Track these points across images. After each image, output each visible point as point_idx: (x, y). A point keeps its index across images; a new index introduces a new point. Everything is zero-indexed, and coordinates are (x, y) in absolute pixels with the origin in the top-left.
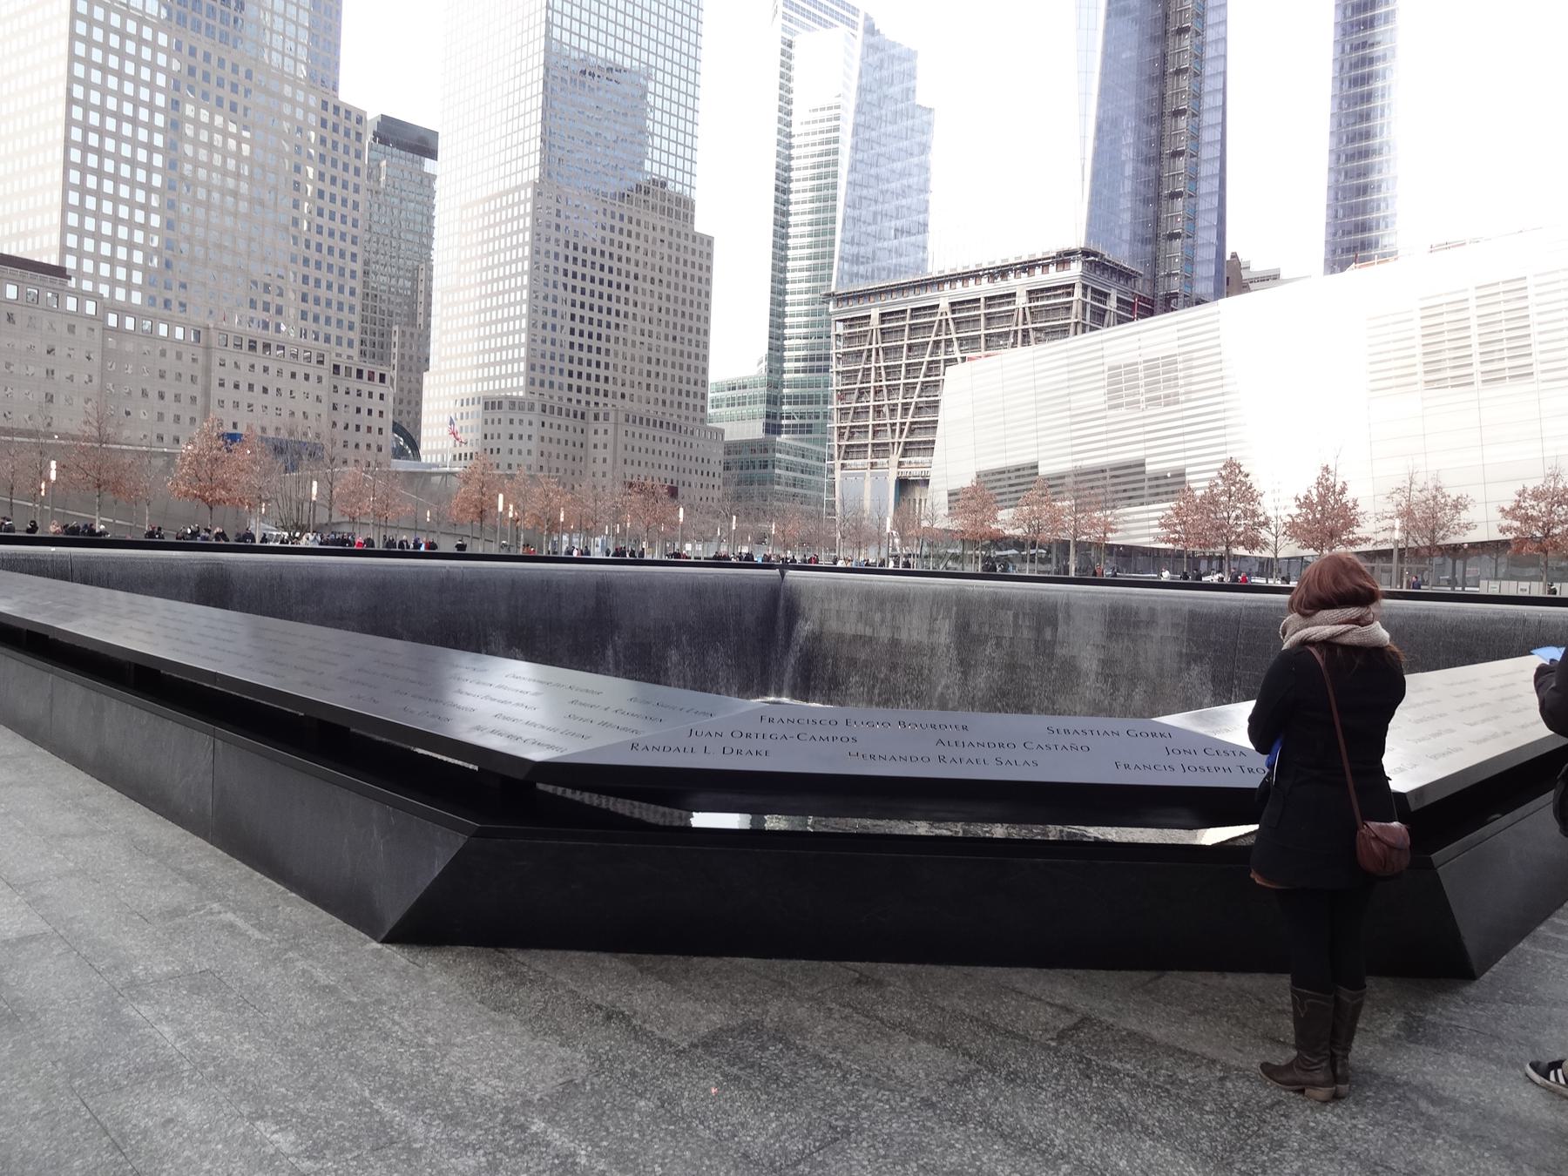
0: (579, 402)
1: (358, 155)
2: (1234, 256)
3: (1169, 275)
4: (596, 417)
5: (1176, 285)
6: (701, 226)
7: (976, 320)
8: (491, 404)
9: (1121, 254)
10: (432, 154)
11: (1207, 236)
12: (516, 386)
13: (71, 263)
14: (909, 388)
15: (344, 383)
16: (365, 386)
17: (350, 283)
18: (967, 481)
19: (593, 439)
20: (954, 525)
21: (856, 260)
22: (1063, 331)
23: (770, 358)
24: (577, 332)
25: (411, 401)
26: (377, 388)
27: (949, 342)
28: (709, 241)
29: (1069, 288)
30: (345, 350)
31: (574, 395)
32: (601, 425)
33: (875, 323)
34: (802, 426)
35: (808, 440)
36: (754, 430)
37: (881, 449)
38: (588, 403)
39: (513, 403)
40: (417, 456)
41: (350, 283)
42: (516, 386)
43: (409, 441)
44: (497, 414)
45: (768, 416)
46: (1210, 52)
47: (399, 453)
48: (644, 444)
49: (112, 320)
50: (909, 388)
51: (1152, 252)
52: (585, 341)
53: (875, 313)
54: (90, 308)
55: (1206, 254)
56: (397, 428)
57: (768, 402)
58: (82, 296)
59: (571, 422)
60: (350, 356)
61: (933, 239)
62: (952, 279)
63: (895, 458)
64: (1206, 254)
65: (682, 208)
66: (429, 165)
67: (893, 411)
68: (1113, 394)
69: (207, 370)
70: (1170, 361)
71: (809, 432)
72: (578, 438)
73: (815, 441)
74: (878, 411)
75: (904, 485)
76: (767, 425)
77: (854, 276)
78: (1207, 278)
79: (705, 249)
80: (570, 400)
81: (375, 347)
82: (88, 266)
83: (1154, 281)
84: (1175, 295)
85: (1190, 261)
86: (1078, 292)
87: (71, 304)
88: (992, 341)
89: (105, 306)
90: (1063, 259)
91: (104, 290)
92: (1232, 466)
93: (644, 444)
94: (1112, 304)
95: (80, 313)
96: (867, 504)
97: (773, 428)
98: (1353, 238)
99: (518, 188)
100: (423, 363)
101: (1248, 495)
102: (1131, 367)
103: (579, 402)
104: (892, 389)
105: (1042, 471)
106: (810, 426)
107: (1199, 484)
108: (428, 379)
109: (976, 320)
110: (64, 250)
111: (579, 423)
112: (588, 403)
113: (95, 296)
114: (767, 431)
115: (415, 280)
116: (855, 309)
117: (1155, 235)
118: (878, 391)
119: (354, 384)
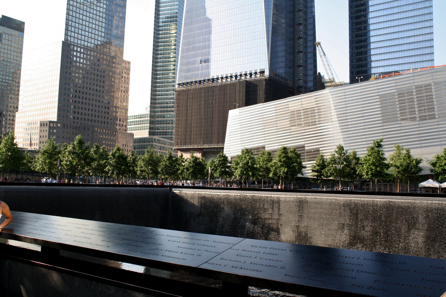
0: (78, 123)
2: (319, 73)
3: (299, 80)
4: (84, 129)
5: (301, 83)
11: (310, 67)
23: (151, 107)
24: (77, 97)
28: (129, 63)
31: (76, 120)
34: (163, 132)
35: (165, 138)
36: (144, 134)
38: (81, 124)
45: (150, 129)
51: (291, 72)
52: (81, 100)
55: (310, 73)
57: (150, 123)
61: (213, 64)
64: (310, 73)
71: (166, 135)
73: (168, 138)
76: (150, 132)
78: (311, 81)
79: (127, 66)
80: (74, 122)
83: (294, 81)
84: (301, 87)
85: (306, 75)
98: (360, 69)
103: (78, 123)
106: (166, 132)
112: (81, 124)
114: (150, 134)
117: (293, 65)
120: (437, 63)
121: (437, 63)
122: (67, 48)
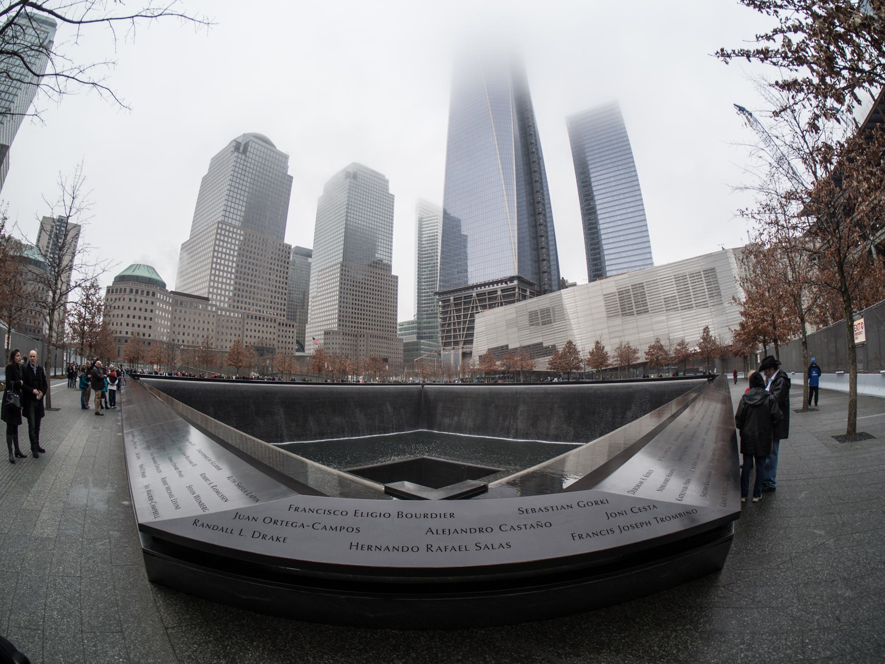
1: (289, 258)
5: (546, 287)
6: (393, 273)
7: (485, 299)
8: (327, 333)
9: (528, 277)
10: (311, 256)
11: (554, 273)
12: (335, 327)
13: (210, 296)
14: (465, 322)
15: (282, 328)
16: (288, 329)
17: (284, 297)
18: (484, 352)
19: (360, 343)
20: (482, 367)
21: (444, 281)
22: (513, 302)
25: (302, 333)
26: (292, 330)
27: (477, 307)
29: (514, 289)
30: (282, 318)
32: (362, 339)
33: (452, 301)
37: (456, 343)
39: (334, 332)
40: (304, 351)
41: (284, 297)
42: (335, 327)
43: (302, 348)
44: (328, 336)
46: (548, 220)
47: (298, 350)
48: (377, 344)
49: (219, 312)
50: (465, 322)
53: (452, 298)
54: (214, 309)
56: (298, 342)
58: (212, 305)
59: (352, 338)
60: (283, 319)
62: (477, 286)
63: (461, 346)
64: (554, 278)
65: (388, 267)
66: (310, 260)
67: (460, 330)
68: (531, 320)
69: (243, 326)
70: (548, 310)
72: (355, 343)
74: (455, 330)
75: (465, 355)
77: (444, 287)
81: (292, 316)
82: (215, 297)
83: (540, 286)
86: (517, 290)
87: (209, 308)
88: (491, 306)
89: (218, 309)
90: (511, 279)
91: (218, 304)
92: (570, 343)
93: (377, 344)
94: (528, 293)
95: (211, 311)
96: (452, 362)
97: (419, 338)
98: (597, 271)
99: (336, 265)
100: (306, 321)
101: (576, 352)
102: (536, 312)
104: (459, 323)
105: (510, 347)
107: (560, 349)
108: (307, 326)
109: (485, 299)
110: (209, 293)
111: (355, 338)
113: (215, 306)
115: (304, 295)
116: (445, 297)
118: (454, 323)
119: (285, 328)
120: (656, 264)
121: (656, 264)
122: (344, 266)
